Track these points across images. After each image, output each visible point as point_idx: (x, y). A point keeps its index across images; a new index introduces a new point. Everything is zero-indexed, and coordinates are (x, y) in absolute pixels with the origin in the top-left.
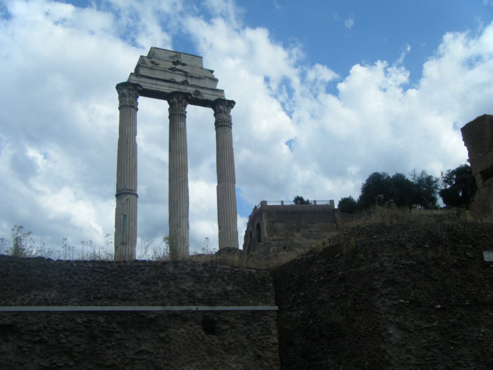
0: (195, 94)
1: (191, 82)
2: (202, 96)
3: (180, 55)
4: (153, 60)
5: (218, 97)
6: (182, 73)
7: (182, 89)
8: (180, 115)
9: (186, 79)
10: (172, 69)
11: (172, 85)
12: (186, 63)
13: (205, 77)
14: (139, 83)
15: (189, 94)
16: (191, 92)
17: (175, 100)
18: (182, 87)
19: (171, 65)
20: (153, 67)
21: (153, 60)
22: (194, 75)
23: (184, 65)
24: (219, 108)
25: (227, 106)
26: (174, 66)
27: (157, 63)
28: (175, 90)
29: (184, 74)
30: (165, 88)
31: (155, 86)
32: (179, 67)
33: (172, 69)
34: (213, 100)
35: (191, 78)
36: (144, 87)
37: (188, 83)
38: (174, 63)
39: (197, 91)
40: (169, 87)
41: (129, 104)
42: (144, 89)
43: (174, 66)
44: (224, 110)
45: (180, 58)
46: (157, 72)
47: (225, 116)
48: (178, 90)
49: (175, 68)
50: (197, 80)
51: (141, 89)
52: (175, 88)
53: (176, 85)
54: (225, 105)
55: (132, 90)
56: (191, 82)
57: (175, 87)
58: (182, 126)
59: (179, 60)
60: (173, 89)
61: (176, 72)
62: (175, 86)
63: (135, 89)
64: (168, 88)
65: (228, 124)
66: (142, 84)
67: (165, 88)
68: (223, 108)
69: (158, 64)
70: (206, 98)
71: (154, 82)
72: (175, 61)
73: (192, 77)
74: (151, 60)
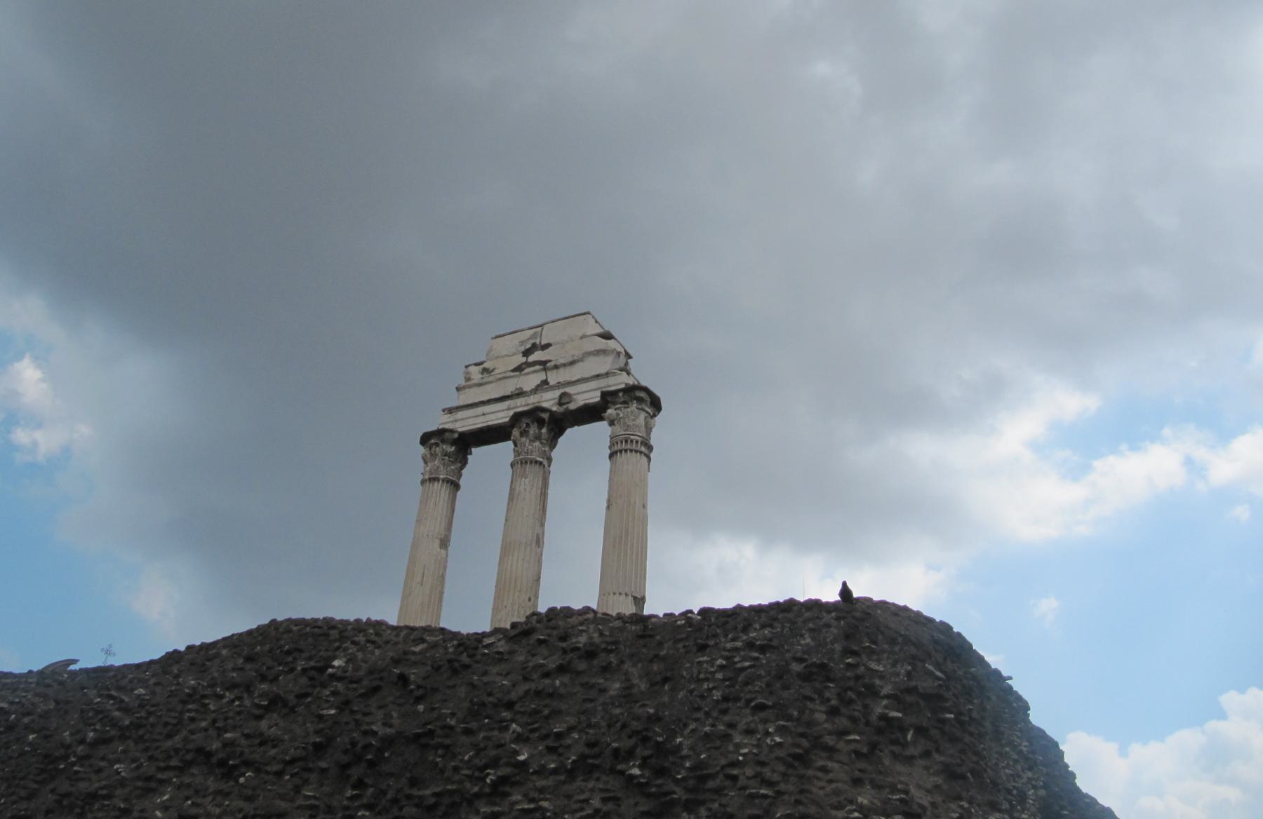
0: (564, 401)
1: (553, 378)
4: (485, 365)
6: (538, 367)
14: (447, 426)
16: (545, 405)
17: (516, 432)
21: (485, 365)
22: (562, 361)
25: (625, 402)
26: (524, 359)
30: (500, 415)
31: (482, 419)
33: (519, 369)
36: (460, 430)
39: (563, 395)
40: (508, 409)
42: (462, 435)
43: (524, 359)
46: (488, 387)
50: (568, 369)
51: (456, 435)
52: (521, 405)
55: (437, 445)
61: (527, 370)
63: (443, 441)
67: (499, 415)
70: (581, 403)
72: (528, 346)
73: (556, 367)
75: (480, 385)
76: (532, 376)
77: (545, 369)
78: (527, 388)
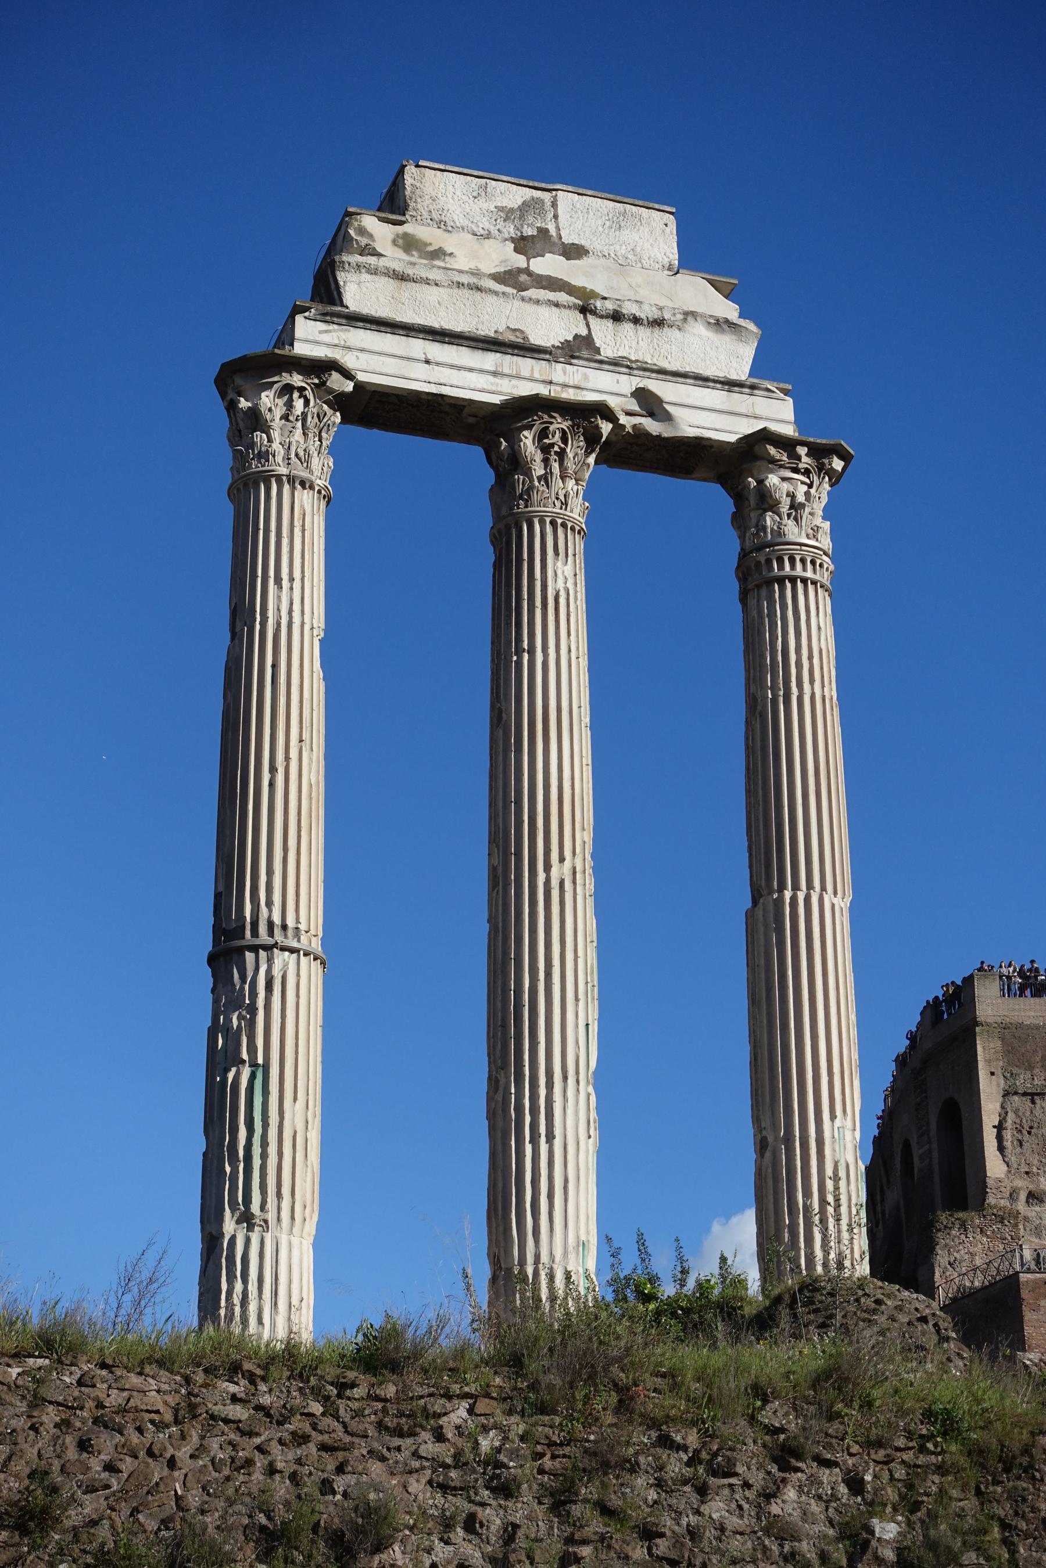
1: (609, 339)
2: (667, 417)
3: (554, 204)
5: (759, 426)
6: (562, 297)
7: (565, 386)
8: (553, 523)
9: (584, 332)
10: (511, 279)
11: (508, 362)
12: (583, 242)
13: (690, 318)
15: (604, 411)
16: (613, 402)
18: (561, 372)
19: (500, 255)
20: (410, 271)
21: (407, 228)
23: (574, 252)
24: (761, 482)
25: (807, 472)
26: (520, 261)
27: (430, 249)
28: (525, 389)
29: (572, 300)
32: (548, 264)
33: (509, 278)
34: (732, 438)
35: (609, 323)
36: (361, 377)
37: (598, 351)
38: (523, 245)
40: (495, 374)
41: (283, 470)
42: (359, 386)
43: (520, 261)
44: (792, 496)
45: (556, 217)
46: (432, 294)
47: (796, 530)
48: (543, 390)
49: (527, 271)
50: (643, 332)
51: (349, 386)
53: (529, 362)
54: (796, 470)
56: (609, 339)
57: (525, 373)
58: (560, 585)
59: (553, 232)
60: (514, 382)
61: (533, 293)
62: (526, 365)
64: (491, 379)
65: (809, 574)
66: (349, 361)
68: (786, 487)
69: (439, 254)
70: (691, 432)
71: (418, 346)
72: (529, 231)
74: (400, 229)
75: (402, 278)
76: (545, 312)
77: (584, 310)
78: (536, 339)
